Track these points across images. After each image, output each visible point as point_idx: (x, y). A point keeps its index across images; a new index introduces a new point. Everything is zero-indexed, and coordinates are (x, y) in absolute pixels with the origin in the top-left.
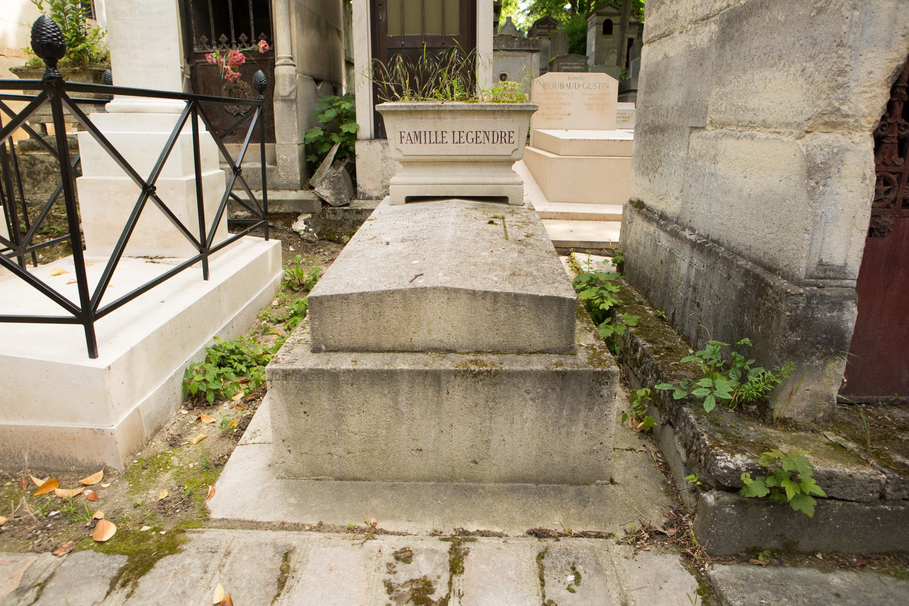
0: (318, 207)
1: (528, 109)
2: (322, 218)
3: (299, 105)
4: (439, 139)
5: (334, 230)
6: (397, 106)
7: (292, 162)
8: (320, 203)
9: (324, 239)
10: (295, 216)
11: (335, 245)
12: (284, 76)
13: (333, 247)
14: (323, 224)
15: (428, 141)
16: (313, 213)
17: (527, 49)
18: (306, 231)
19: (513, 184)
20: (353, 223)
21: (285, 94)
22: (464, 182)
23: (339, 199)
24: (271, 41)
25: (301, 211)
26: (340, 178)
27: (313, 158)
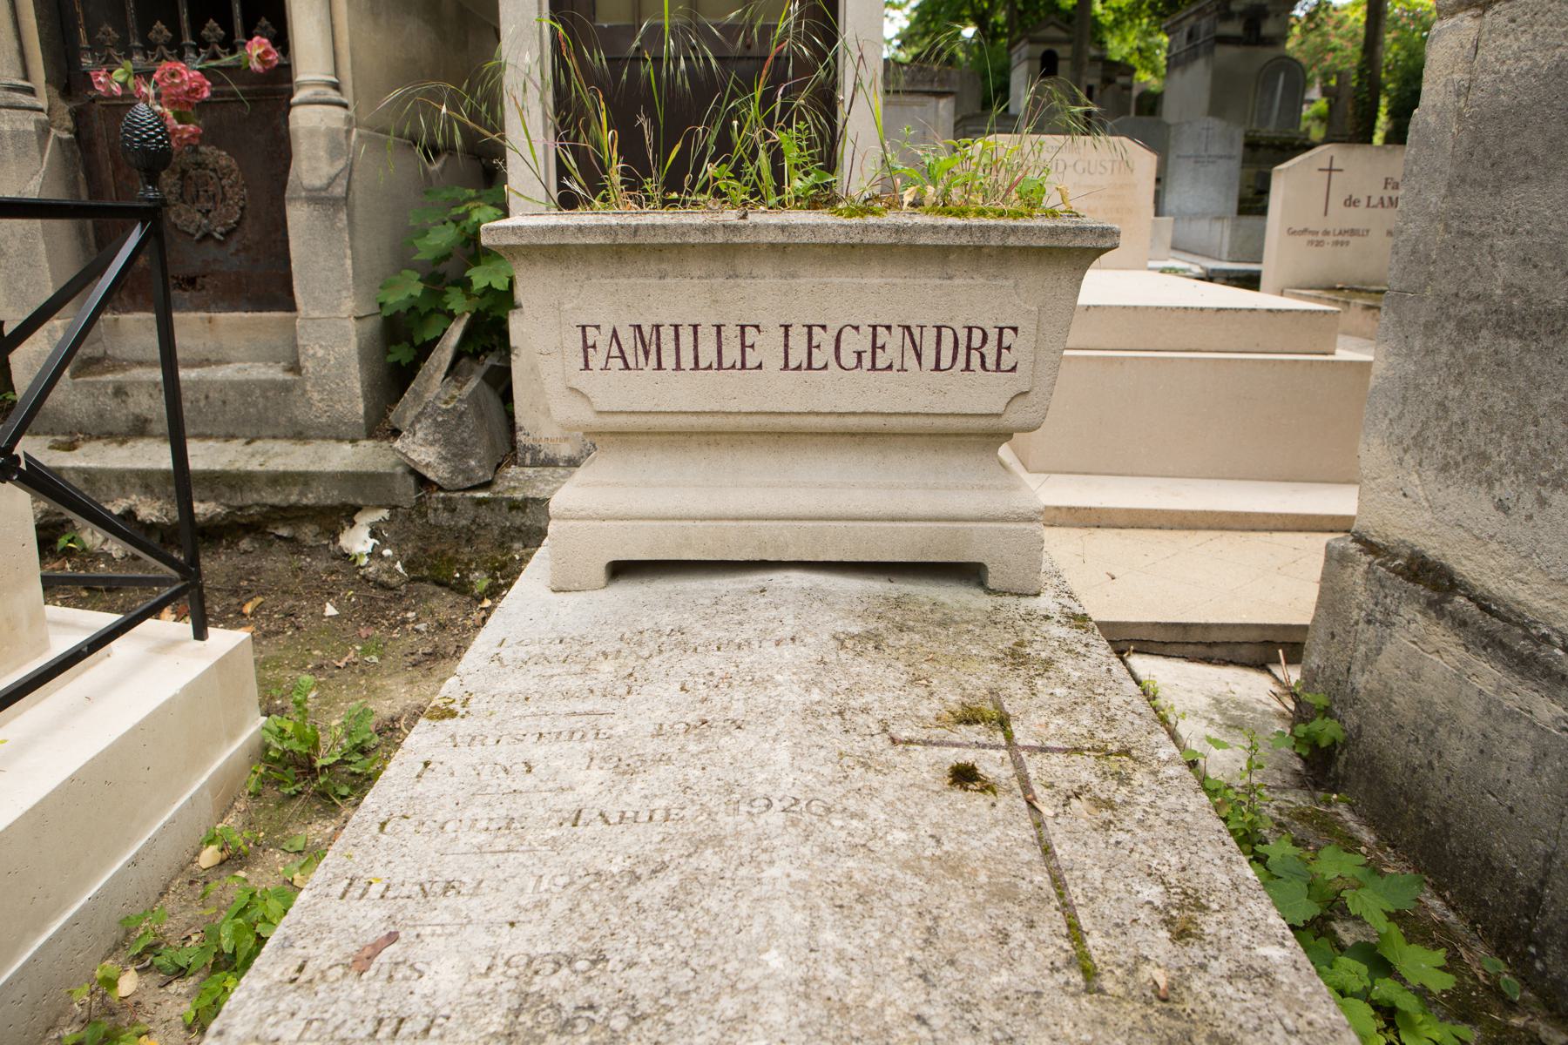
0: (406, 493)
1: (1078, 242)
2: (418, 521)
3: (359, 213)
4: (732, 354)
5: (451, 553)
6: (563, 229)
7: (341, 365)
8: (411, 480)
9: (422, 579)
10: (348, 514)
11: (451, 598)
12: (312, 133)
13: (444, 604)
14: (421, 538)
15: (687, 359)
16: (393, 508)
17: (927, 88)
18: (375, 554)
19: (1004, 519)
20: (503, 534)
21: (318, 183)
22: (822, 511)
23: (463, 471)
24: (282, 40)
25: (360, 502)
26: (462, 414)
27: (402, 354)
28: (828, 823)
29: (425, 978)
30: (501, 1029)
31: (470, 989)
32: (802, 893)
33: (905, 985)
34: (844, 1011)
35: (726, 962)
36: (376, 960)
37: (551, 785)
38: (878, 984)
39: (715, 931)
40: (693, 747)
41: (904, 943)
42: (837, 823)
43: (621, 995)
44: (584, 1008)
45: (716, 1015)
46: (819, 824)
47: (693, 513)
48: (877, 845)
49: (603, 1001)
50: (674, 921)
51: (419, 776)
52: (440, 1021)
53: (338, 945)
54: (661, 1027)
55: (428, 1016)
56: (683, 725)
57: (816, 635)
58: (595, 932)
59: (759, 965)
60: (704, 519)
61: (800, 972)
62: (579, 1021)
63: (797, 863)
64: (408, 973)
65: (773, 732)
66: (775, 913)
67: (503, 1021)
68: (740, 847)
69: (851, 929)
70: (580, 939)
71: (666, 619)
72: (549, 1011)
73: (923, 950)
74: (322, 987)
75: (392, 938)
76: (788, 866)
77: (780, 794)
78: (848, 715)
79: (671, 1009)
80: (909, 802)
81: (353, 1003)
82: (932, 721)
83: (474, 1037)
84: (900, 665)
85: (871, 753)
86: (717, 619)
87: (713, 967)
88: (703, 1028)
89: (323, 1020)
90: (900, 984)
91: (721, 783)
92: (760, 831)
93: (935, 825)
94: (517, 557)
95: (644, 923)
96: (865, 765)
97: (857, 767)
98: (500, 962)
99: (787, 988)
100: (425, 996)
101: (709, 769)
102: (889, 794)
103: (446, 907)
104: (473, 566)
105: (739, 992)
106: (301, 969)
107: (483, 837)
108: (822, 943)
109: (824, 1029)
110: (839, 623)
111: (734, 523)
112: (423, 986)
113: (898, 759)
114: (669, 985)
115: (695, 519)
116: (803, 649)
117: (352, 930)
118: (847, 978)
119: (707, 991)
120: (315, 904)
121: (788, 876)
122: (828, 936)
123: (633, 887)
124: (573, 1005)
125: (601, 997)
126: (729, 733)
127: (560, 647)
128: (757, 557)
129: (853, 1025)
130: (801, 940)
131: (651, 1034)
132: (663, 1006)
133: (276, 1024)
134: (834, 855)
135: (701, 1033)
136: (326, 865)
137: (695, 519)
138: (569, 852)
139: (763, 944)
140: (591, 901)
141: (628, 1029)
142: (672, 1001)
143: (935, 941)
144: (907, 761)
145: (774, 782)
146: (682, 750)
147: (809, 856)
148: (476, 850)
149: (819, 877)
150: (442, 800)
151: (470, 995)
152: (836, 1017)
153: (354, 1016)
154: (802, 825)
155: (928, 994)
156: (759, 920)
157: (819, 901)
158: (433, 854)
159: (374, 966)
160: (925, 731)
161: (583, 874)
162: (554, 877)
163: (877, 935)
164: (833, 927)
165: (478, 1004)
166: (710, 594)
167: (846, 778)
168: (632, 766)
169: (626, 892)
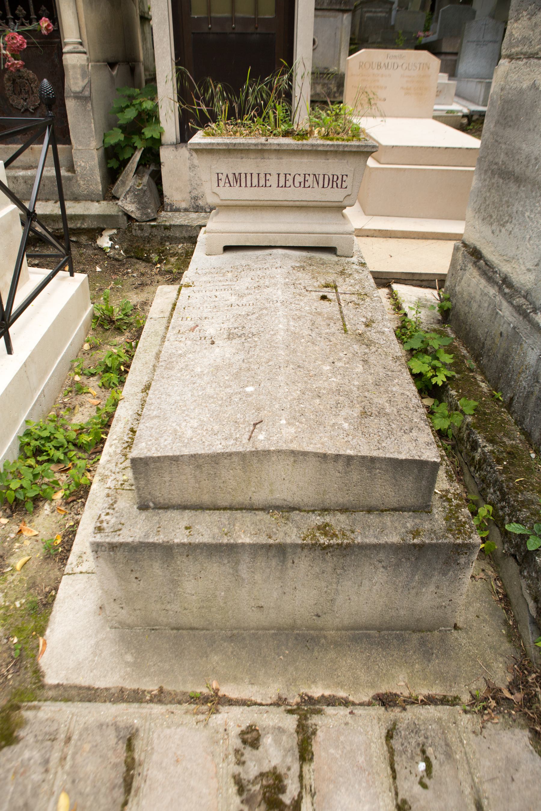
0: (123, 222)
1: (366, 150)
2: (129, 234)
3: (94, 101)
4: (262, 182)
5: (142, 247)
6: (213, 144)
7: (91, 170)
8: (125, 218)
9: (131, 257)
10: (100, 231)
11: (144, 264)
12: (74, 67)
13: (142, 266)
14: (130, 241)
15: (249, 184)
16: (118, 229)
17: (338, 7)
18: (112, 247)
19: (342, 234)
20: (161, 239)
21: (78, 90)
22: (288, 231)
23: (146, 214)
24: (54, 18)
25: (105, 226)
26: (145, 191)
27: (114, 164)
40: (257, 291)
115: (250, 233)
119: (267, 331)
128: (269, 245)
137: (250, 233)
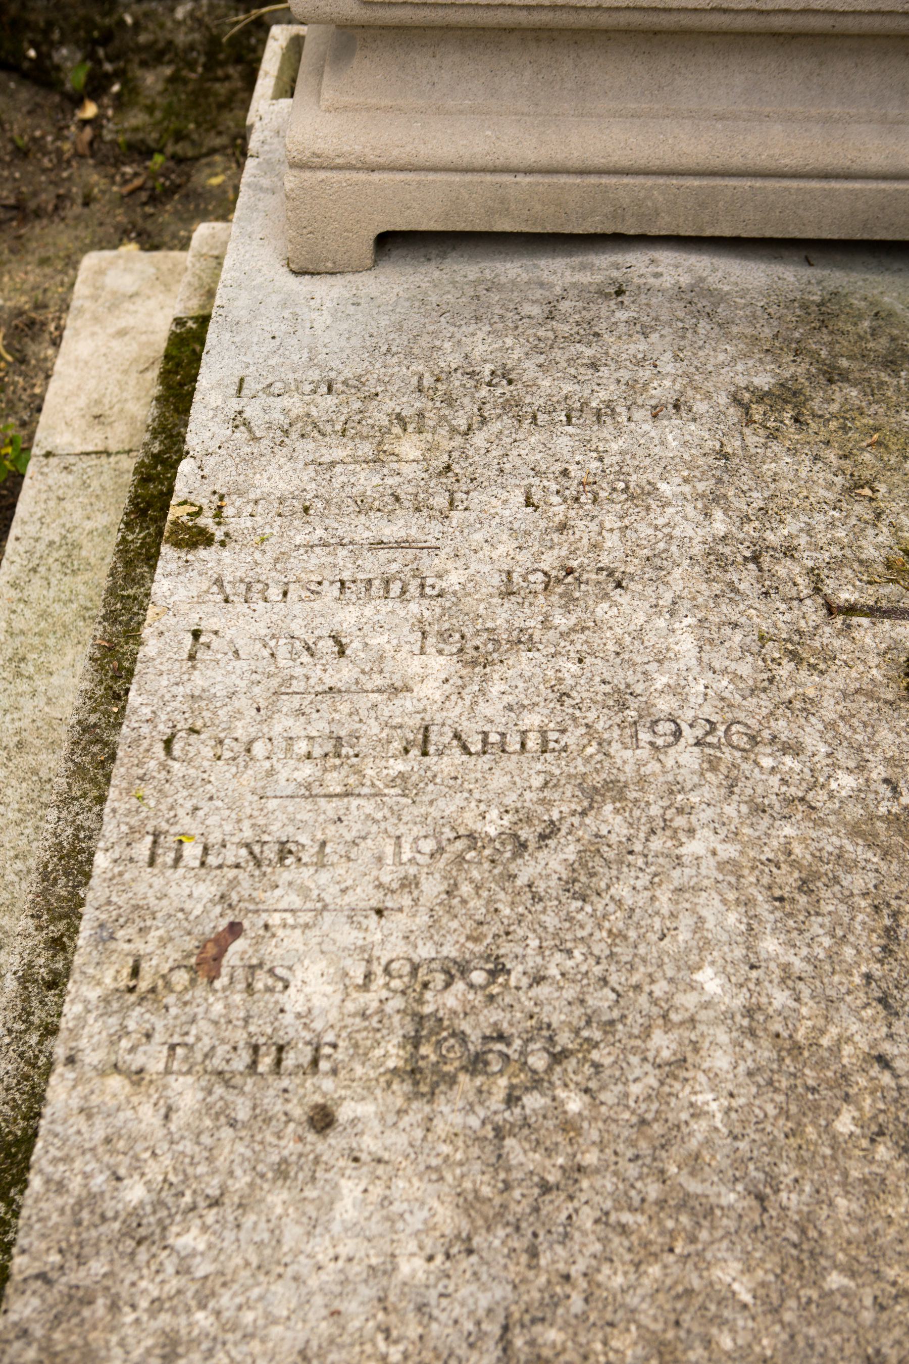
22: (716, 163)
28: (756, 763)
29: (292, 990)
30: (401, 1063)
31: (350, 1007)
32: (733, 880)
33: (863, 1013)
34: (795, 1052)
35: (653, 982)
36: (224, 962)
37: (378, 681)
38: (832, 1012)
39: (632, 934)
40: (560, 620)
41: (859, 952)
42: (767, 762)
43: (533, 1022)
44: (491, 1038)
45: (650, 1055)
46: (744, 766)
47: (515, 162)
48: (818, 797)
49: (513, 1030)
50: (580, 917)
51: (192, 657)
52: (327, 1050)
53: (171, 939)
54: (588, 1070)
55: (309, 1043)
56: (540, 576)
57: (708, 396)
58: (485, 928)
59: (693, 988)
60: (529, 171)
61: (739, 1001)
62: (490, 1056)
63: (723, 832)
64: (270, 982)
65: (668, 596)
66: (704, 912)
67: (401, 1053)
68: (648, 804)
69: (795, 934)
70: (468, 938)
71: (479, 351)
72: (452, 1041)
73: (881, 961)
74: (171, 999)
75: (235, 930)
76: (712, 838)
77: (689, 714)
78: (766, 560)
79: (596, 1045)
80: (855, 722)
81: (216, 1023)
82: (881, 569)
83: (372, 1074)
84: (831, 456)
85: (799, 632)
86: (557, 354)
87: (637, 988)
88: (638, 1072)
89: (186, 1045)
90: (855, 1012)
91: (607, 688)
92: (670, 778)
93: (890, 761)
94: (129, 20)
95: (543, 918)
96: (794, 656)
97: (784, 661)
98: (378, 969)
99: (729, 1022)
100: (299, 1016)
101: (588, 660)
102: (830, 709)
103: (290, 884)
104: (56, 35)
105: (674, 1025)
106: (135, 972)
107: (307, 771)
108: (763, 955)
109: (776, 1077)
110: (740, 367)
111: (578, 180)
112: (293, 1001)
113: (837, 643)
114: (589, 1011)
115: (515, 171)
116: (693, 427)
117: (180, 915)
118: (795, 1005)
119: (635, 1022)
120: (121, 874)
121: (714, 853)
122: (770, 945)
123: (519, 861)
124: (478, 1033)
125: (511, 1024)
126: (606, 596)
127: (331, 400)
128: (609, 229)
129: (807, 1071)
130: (739, 952)
131: (578, 1078)
132: (587, 1040)
133: (132, 1050)
134: (766, 817)
135: (636, 1080)
136: (114, 811)
137: (515, 171)
138: (426, 799)
139: (694, 958)
140: (472, 881)
141: (549, 1069)
142: (597, 1035)
143: (895, 948)
144: (850, 647)
145: (676, 690)
146: (546, 623)
147: (736, 821)
148: (303, 791)
149: (752, 854)
150: (237, 704)
151: (354, 1015)
152: (788, 1061)
153: (223, 1041)
154: (723, 769)
155: (890, 1026)
156: (686, 921)
157: (753, 891)
158: (249, 797)
159: (225, 971)
160: (871, 590)
161: (452, 835)
162: (416, 839)
163: (827, 941)
164: (774, 930)
165: (366, 1029)
166: (538, 294)
167: (771, 680)
168: (482, 649)
169: (513, 868)
